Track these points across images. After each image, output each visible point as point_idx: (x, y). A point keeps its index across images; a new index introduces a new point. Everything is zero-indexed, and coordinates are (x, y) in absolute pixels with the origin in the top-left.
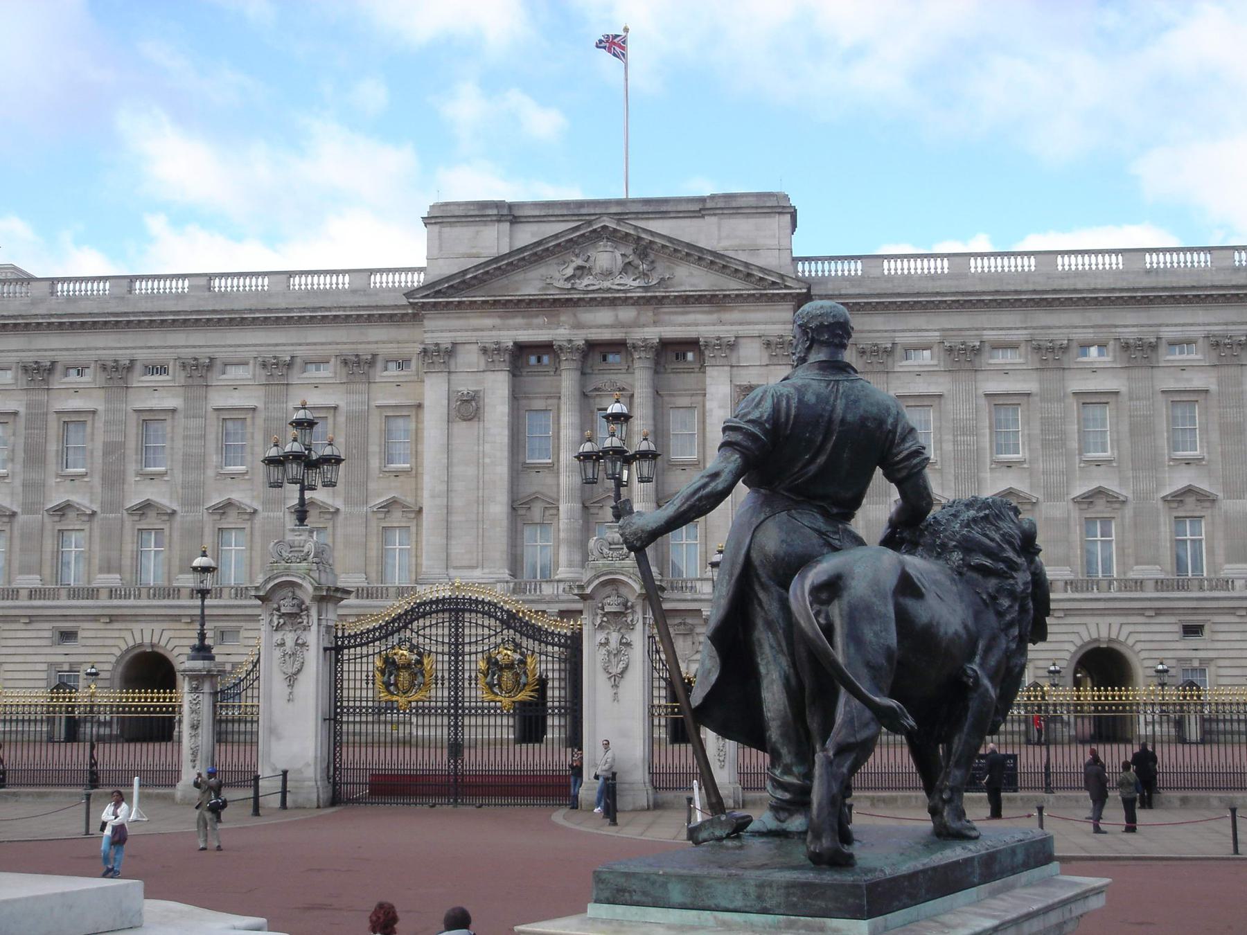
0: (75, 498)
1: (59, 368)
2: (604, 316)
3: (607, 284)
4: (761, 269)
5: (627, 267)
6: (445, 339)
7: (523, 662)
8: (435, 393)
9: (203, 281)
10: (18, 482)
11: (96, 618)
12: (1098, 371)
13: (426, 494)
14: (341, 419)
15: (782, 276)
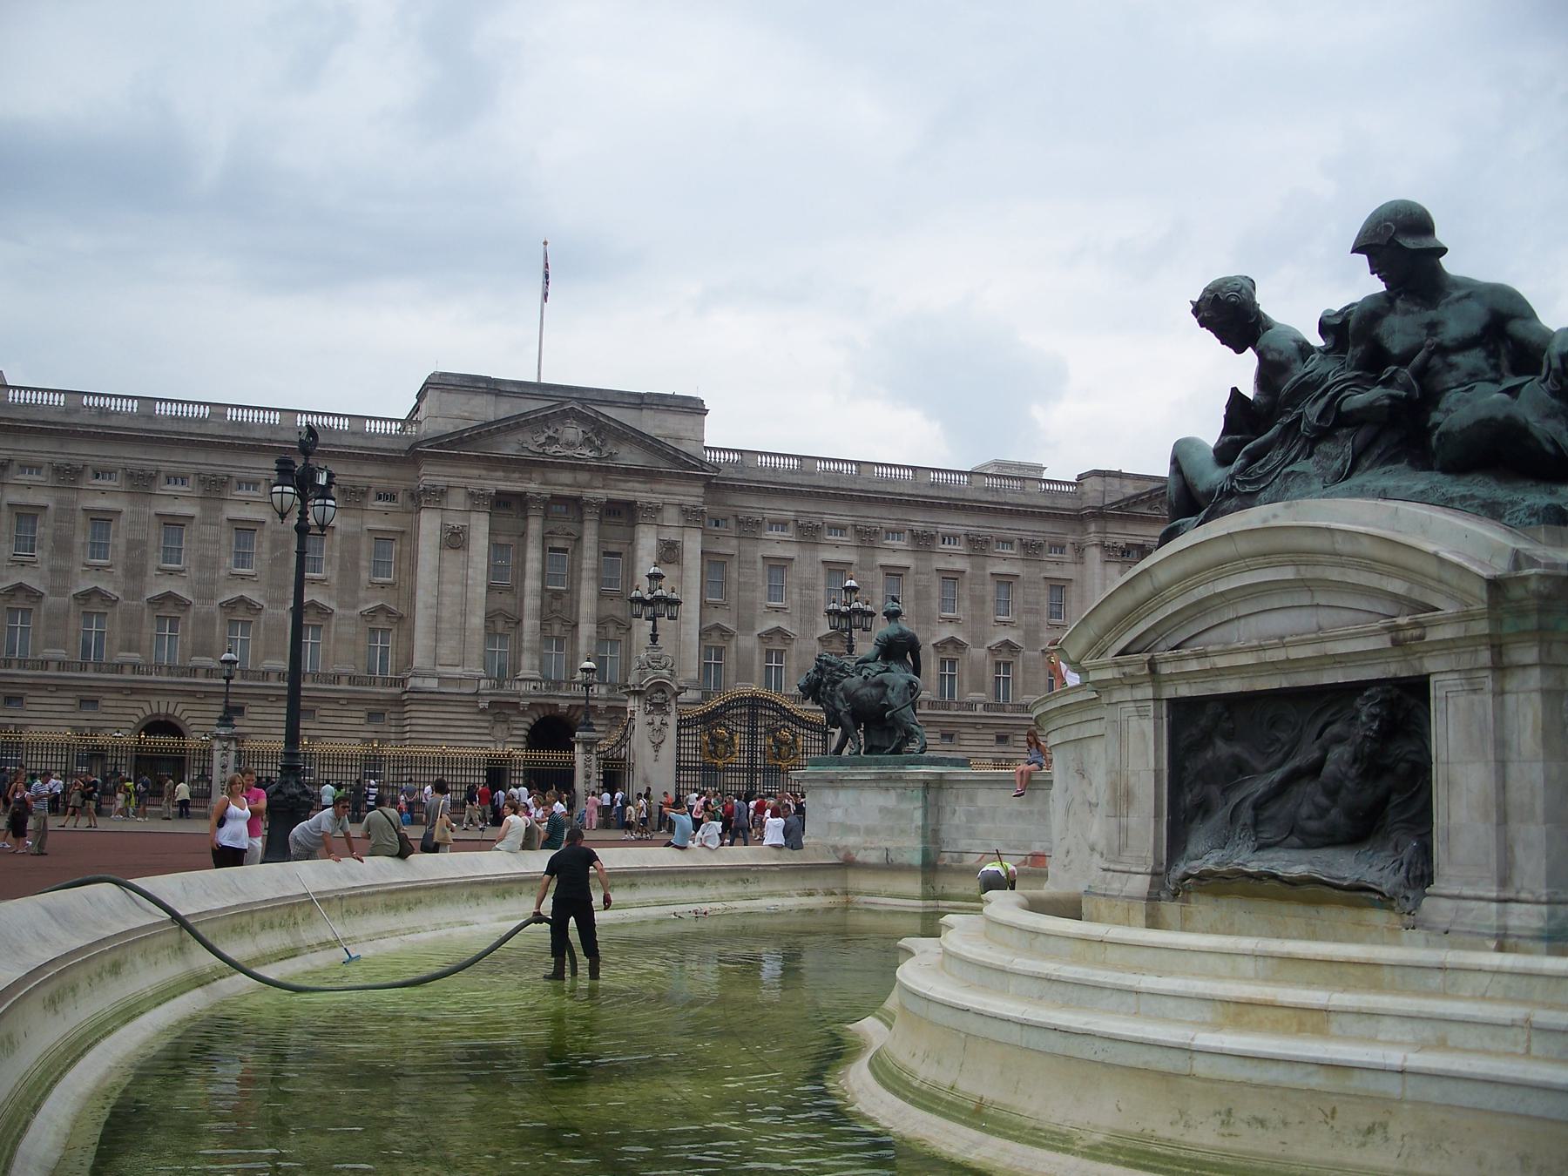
0: (102, 586)
1: (89, 471)
2: (566, 477)
3: (569, 453)
4: (687, 455)
5: (587, 442)
6: (441, 481)
7: (795, 741)
8: (429, 525)
9: (221, 410)
10: (45, 568)
11: (119, 690)
12: (897, 554)
13: (419, 605)
14: (337, 538)
15: (701, 462)
